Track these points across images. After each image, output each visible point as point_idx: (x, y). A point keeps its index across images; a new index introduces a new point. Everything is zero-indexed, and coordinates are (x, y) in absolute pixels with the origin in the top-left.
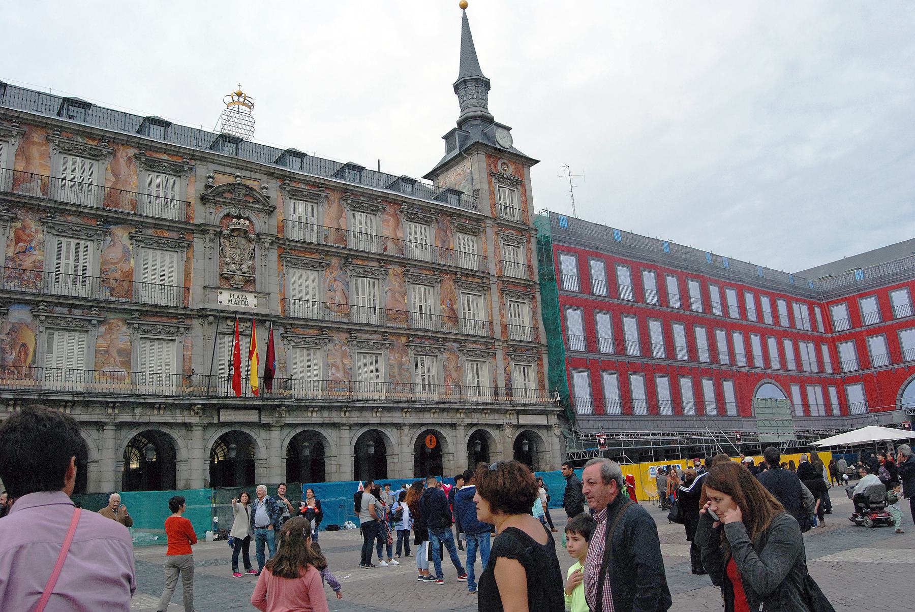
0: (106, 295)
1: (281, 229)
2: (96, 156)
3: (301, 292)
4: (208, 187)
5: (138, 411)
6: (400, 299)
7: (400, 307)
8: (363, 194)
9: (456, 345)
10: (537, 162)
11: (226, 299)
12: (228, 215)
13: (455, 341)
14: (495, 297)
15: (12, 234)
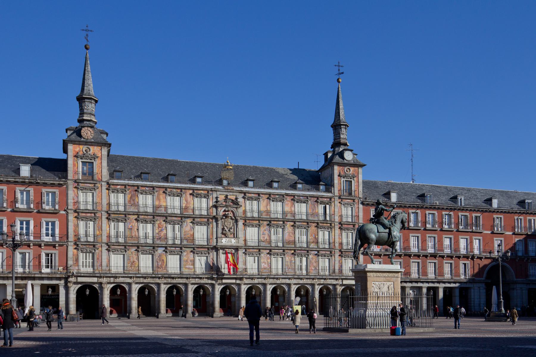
0: (185, 242)
1: (245, 212)
2: (180, 195)
3: (252, 236)
4: (217, 202)
5: (197, 279)
6: (292, 235)
7: (292, 239)
8: (277, 195)
9: (316, 252)
10: (365, 165)
11: (224, 241)
12: (225, 211)
13: (316, 251)
14: (337, 231)
15: (157, 225)
